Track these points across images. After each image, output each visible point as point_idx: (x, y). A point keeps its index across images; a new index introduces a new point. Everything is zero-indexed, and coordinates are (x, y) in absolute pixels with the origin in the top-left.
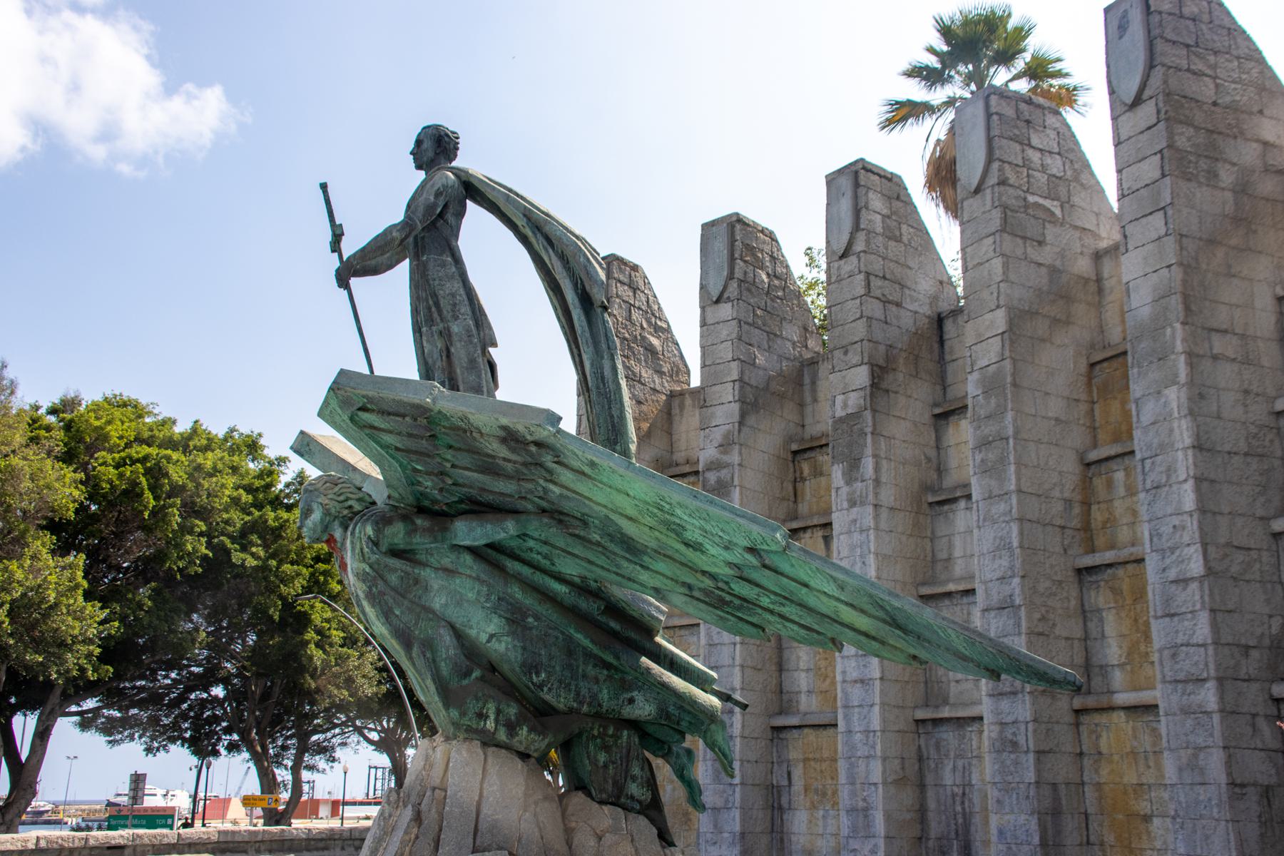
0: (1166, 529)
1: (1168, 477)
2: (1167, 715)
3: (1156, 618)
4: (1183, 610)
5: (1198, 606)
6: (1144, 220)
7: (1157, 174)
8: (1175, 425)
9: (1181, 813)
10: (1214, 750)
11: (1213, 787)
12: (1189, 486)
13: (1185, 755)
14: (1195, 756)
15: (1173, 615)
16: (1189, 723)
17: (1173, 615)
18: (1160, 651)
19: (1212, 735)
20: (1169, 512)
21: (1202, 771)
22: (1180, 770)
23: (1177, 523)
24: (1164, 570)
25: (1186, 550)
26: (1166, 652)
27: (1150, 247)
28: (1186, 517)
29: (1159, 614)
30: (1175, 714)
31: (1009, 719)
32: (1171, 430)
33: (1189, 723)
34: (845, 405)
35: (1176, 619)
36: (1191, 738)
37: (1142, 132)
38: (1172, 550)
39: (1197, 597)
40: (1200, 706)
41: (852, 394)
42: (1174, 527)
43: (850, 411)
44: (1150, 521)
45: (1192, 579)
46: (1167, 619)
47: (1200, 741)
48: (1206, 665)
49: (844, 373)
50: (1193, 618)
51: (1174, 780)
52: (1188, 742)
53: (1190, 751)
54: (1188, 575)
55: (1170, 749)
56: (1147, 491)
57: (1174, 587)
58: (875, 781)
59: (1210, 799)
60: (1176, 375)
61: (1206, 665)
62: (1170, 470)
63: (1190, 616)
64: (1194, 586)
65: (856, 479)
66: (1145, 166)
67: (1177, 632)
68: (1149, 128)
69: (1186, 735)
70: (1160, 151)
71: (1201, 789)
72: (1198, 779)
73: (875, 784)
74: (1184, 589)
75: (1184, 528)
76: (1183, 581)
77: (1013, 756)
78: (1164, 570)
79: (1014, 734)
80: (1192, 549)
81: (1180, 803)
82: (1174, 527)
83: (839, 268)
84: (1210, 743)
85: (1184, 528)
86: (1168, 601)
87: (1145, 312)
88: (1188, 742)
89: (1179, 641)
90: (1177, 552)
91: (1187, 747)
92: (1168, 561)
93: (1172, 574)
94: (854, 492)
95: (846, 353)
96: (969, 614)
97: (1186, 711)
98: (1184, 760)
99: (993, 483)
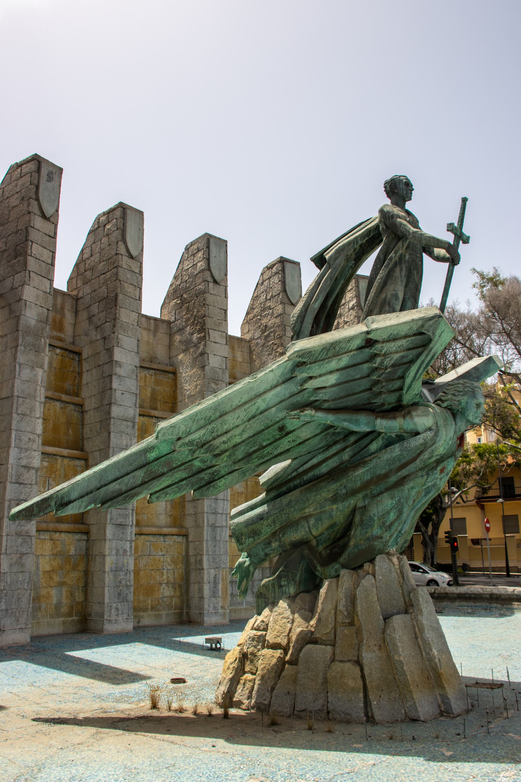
0: (25, 438)
1: (31, 412)
2: (7, 535)
3: (11, 483)
4: (26, 482)
5: (34, 482)
6: (40, 277)
8: (39, 388)
9: (7, 588)
10: (31, 555)
12: (40, 421)
13: (15, 558)
14: (21, 558)
15: (20, 484)
16: (20, 540)
17: (20, 484)
18: (10, 501)
19: (31, 548)
20: (28, 430)
21: (23, 565)
22: (11, 565)
23: (32, 438)
24: (19, 459)
25: (33, 453)
26: (13, 502)
28: (36, 436)
29: (13, 481)
30: (12, 536)
32: (36, 390)
33: (20, 540)
35: (22, 486)
36: (20, 548)
38: (27, 450)
39: (34, 478)
40: (27, 532)
42: (29, 439)
44: (16, 430)
45: (33, 468)
46: (17, 485)
47: (24, 550)
50: (31, 488)
51: (7, 570)
52: (17, 550)
53: (18, 555)
54: (32, 465)
55: (6, 553)
56: (18, 414)
57: (23, 469)
59: (24, 580)
60: (43, 364)
62: (32, 409)
63: (29, 486)
64: (34, 471)
67: (21, 493)
69: (17, 547)
71: (20, 575)
72: (21, 570)
74: (28, 472)
75: (34, 441)
76: (28, 468)
78: (19, 459)
80: (37, 453)
81: (7, 582)
82: (29, 439)
84: (29, 551)
85: (34, 441)
86: (19, 476)
87: (33, 323)
88: (17, 550)
89: (21, 498)
90: (29, 452)
92: (23, 455)
93: (24, 462)
97: (18, 534)
98: (14, 560)
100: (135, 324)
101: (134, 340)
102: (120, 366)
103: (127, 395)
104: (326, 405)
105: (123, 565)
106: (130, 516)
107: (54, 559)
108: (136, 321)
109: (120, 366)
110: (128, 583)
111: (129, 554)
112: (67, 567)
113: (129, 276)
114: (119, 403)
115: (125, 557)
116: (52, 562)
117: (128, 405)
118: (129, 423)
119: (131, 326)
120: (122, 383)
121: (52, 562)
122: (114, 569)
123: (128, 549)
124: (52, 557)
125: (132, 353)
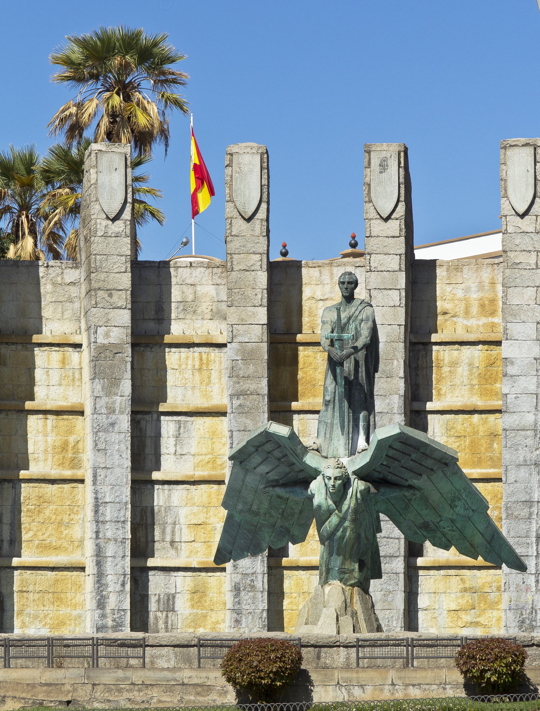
6: (385, 292)
7: (397, 268)
11: (395, 611)
27: (388, 309)
31: (250, 571)
34: (107, 335)
37: (388, 237)
41: (114, 329)
43: (112, 341)
47: (391, 588)
48: (399, 549)
49: (107, 311)
58: (124, 608)
61: (399, 549)
65: (116, 394)
66: (389, 258)
68: (393, 237)
70: (400, 255)
73: (124, 610)
77: (251, 594)
79: (252, 581)
83: (106, 226)
91: (381, 591)
94: (114, 403)
95: (110, 295)
96: (169, 496)
99: (248, 421)
100: (532, 303)
101: (530, 325)
102: (512, 363)
103: (524, 398)
104: (281, 482)
105: (526, 603)
106: (534, 545)
107: (463, 597)
108: (534, 298)
109: (512, 363)
110: (534, 623)
111: (534, 589)
112: (482, 605)
113: (517, 242)
114: (512, 410)
115: (529, 593)
116: (460, 601)
117: (525, 409)
118: (529, 432)
119: (525, 307)
120: (516, 385)
121: (460, 601)
122: (513, 607)
123: (533, 584)
124: (459, 594)
125: (529, 342)
